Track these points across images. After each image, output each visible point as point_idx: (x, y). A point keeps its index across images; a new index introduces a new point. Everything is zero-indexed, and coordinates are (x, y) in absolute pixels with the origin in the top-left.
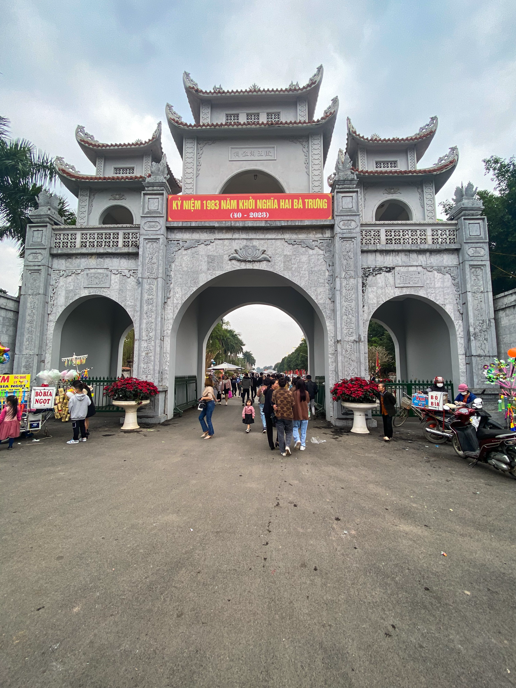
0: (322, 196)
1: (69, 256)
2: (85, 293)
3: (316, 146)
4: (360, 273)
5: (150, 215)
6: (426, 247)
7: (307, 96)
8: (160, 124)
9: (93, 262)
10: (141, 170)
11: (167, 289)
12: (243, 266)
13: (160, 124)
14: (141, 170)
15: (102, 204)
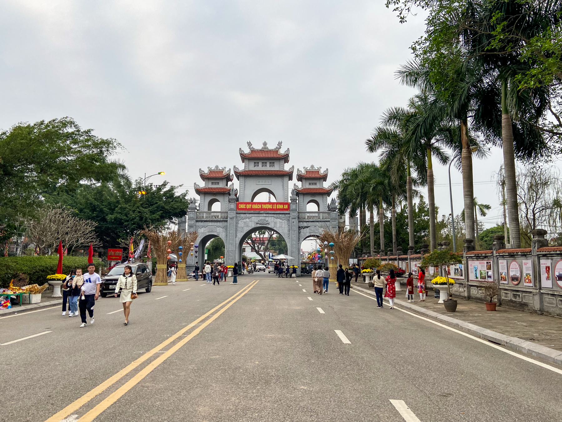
0: (287, 203)
1: (202, 221)
2: (208, 234)
3: (286, 179)
4: (297, 229)
5: (231, 210)
6: (319, 220)
7: (285, 158)
8: (230, 169)
9: (210, 224)
10: (222, 185)
11: (236, 233)
12: (261, 225)
13: (230, 169)
14: (222, 185)
15: (209, 198)
